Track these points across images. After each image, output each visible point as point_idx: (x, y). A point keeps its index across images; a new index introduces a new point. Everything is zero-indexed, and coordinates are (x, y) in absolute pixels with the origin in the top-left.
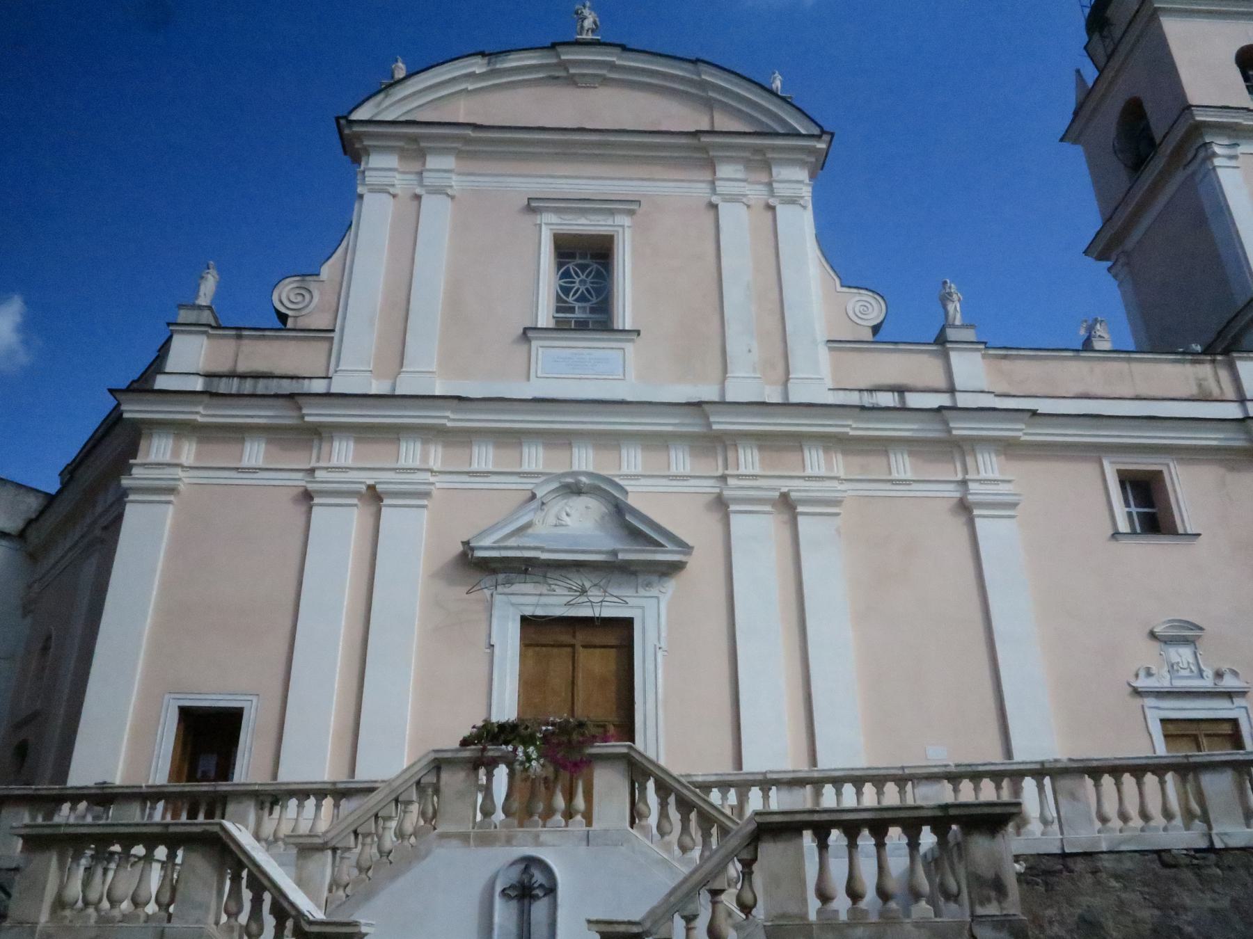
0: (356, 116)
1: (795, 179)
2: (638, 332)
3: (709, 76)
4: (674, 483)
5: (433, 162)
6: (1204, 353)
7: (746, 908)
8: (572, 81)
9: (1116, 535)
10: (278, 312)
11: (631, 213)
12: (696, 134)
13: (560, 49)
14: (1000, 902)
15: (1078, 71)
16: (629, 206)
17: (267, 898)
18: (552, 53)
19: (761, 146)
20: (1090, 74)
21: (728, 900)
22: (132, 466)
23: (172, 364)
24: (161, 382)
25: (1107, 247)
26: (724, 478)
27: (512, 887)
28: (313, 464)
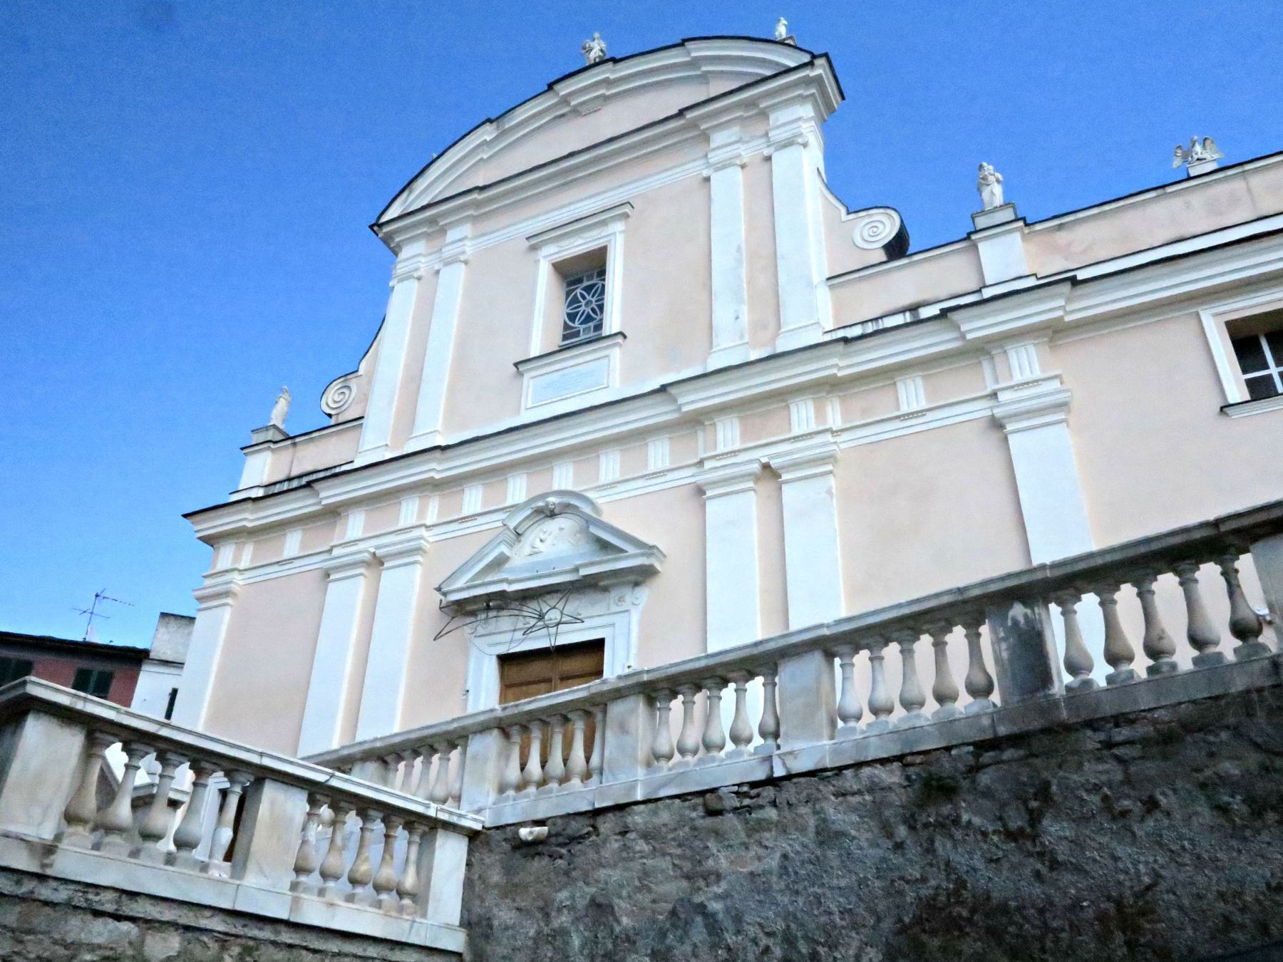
1: (799, 118)
3: (699, 50)
4: (653, 481)
8: (576, 112)
9: (1225, 408)
11: (626, 216)
12: (681, 113)
13: (557, 87)
16: (621, 211)
18: (550, 94)
19: (751, 96)
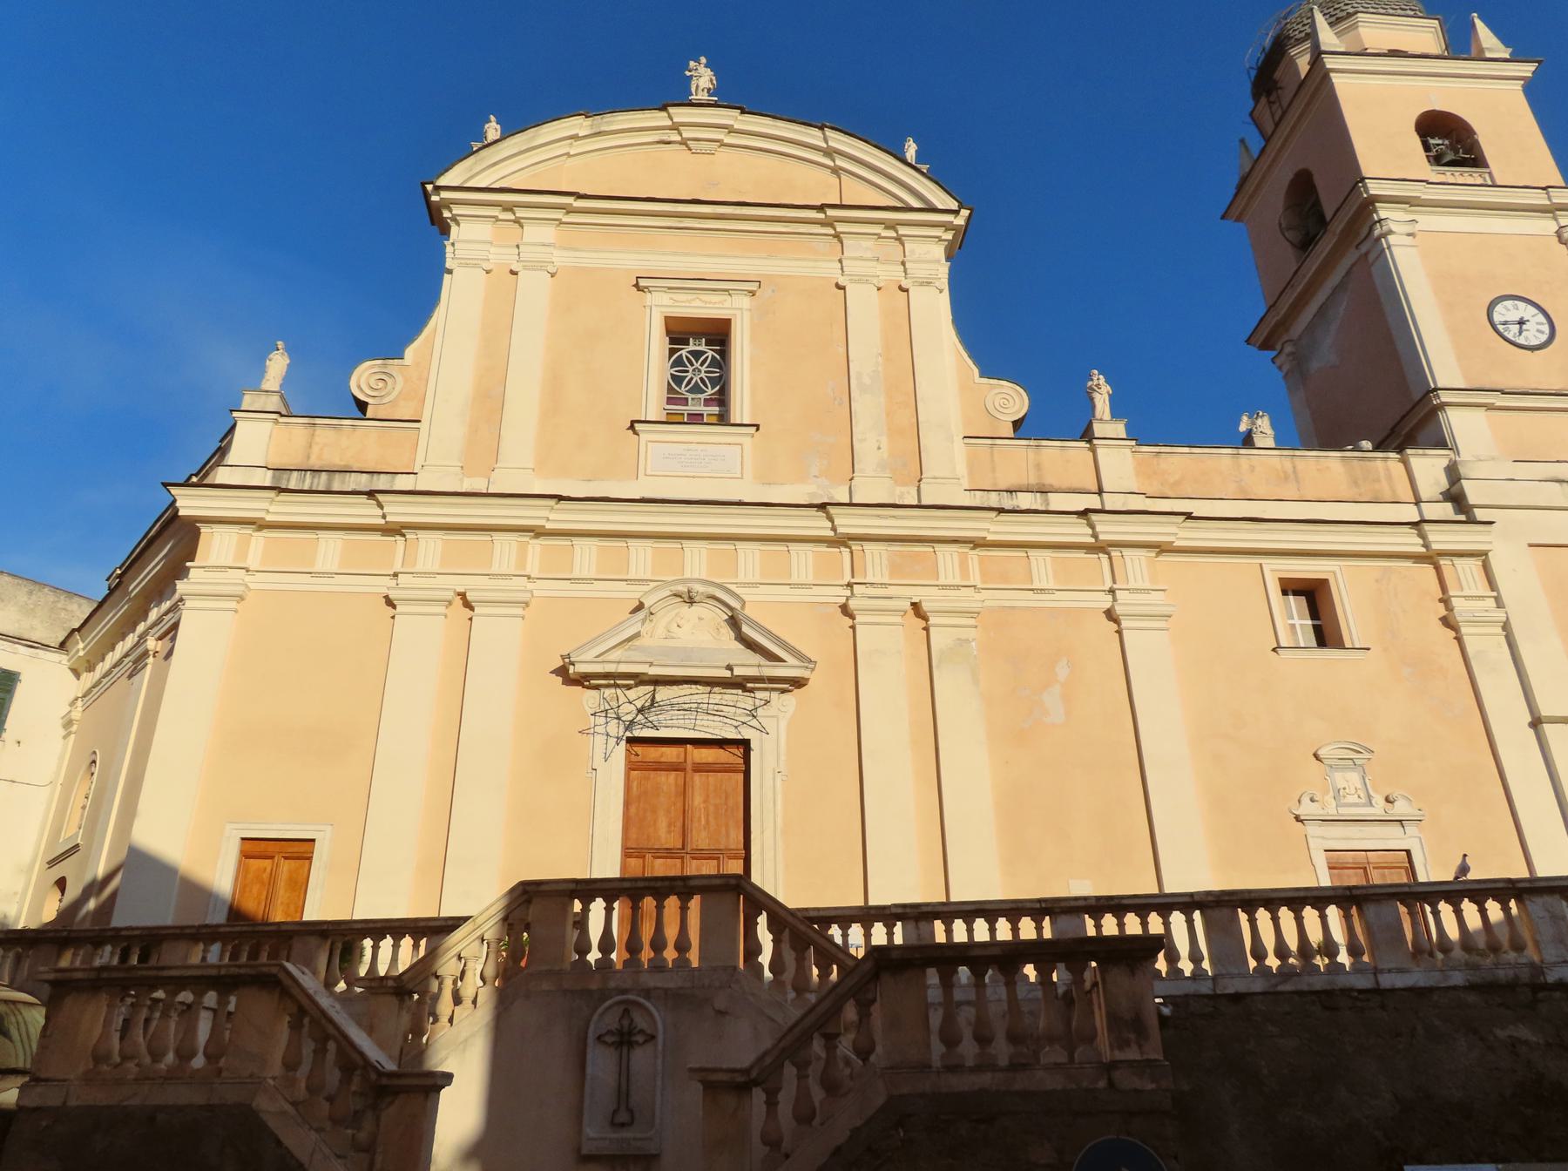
0: (442, 182)
2: (757, 427)
5: (532, 233)
6: (1377, 448)
7: (864, 1053)
10: (355, 398)
11: (753, 293)
12: (821, 208)
14: (1140, 1046)
15: (1242, 141)
17: (332, 1046)
20: (1256, 143)
21: (845, 1046)
22: (188, 569)
23: (231, 458)
24: (222, 475)
25: (1267, 338)
26: (850, 585)
27: (609, 1032)
28: (398, 568)
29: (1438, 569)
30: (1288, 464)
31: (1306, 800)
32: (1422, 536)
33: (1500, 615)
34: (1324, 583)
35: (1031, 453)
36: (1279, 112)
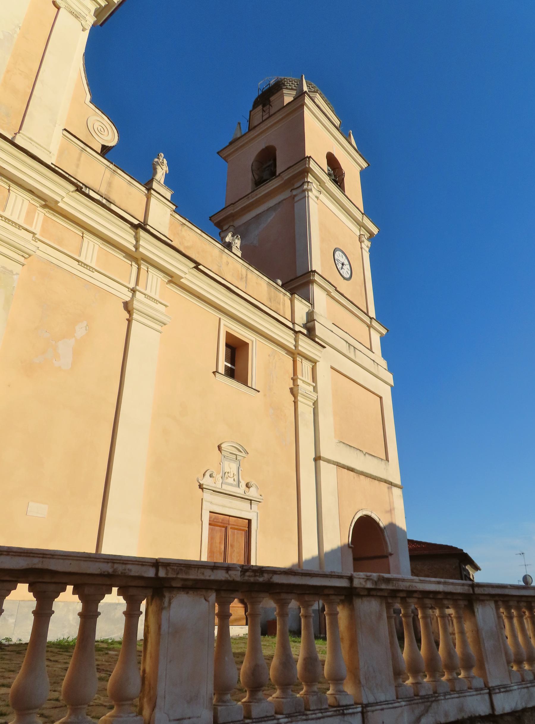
6: (282, 286)
15: (239, 124)
20: (245, 129)
29: (295, 362)
30: (244, 271)
31: (208, 474)
32: (296, 340)
33: (314, 396)
34: (246, 345)
35: (108, 173)
36: (267, 116)
